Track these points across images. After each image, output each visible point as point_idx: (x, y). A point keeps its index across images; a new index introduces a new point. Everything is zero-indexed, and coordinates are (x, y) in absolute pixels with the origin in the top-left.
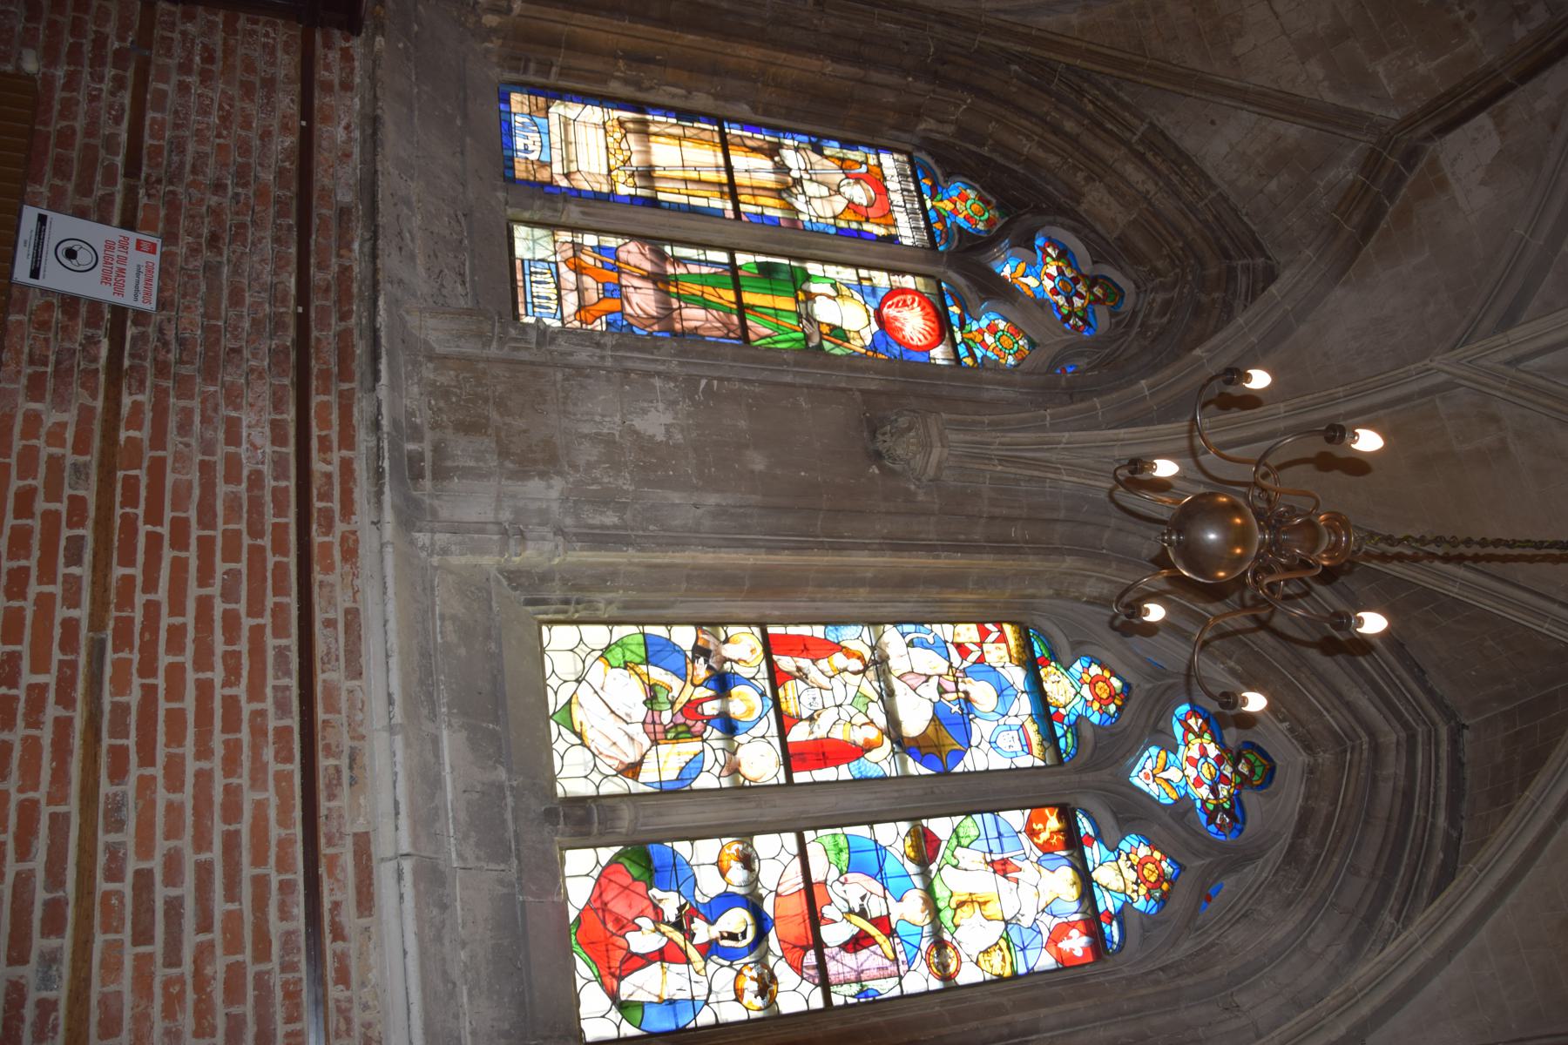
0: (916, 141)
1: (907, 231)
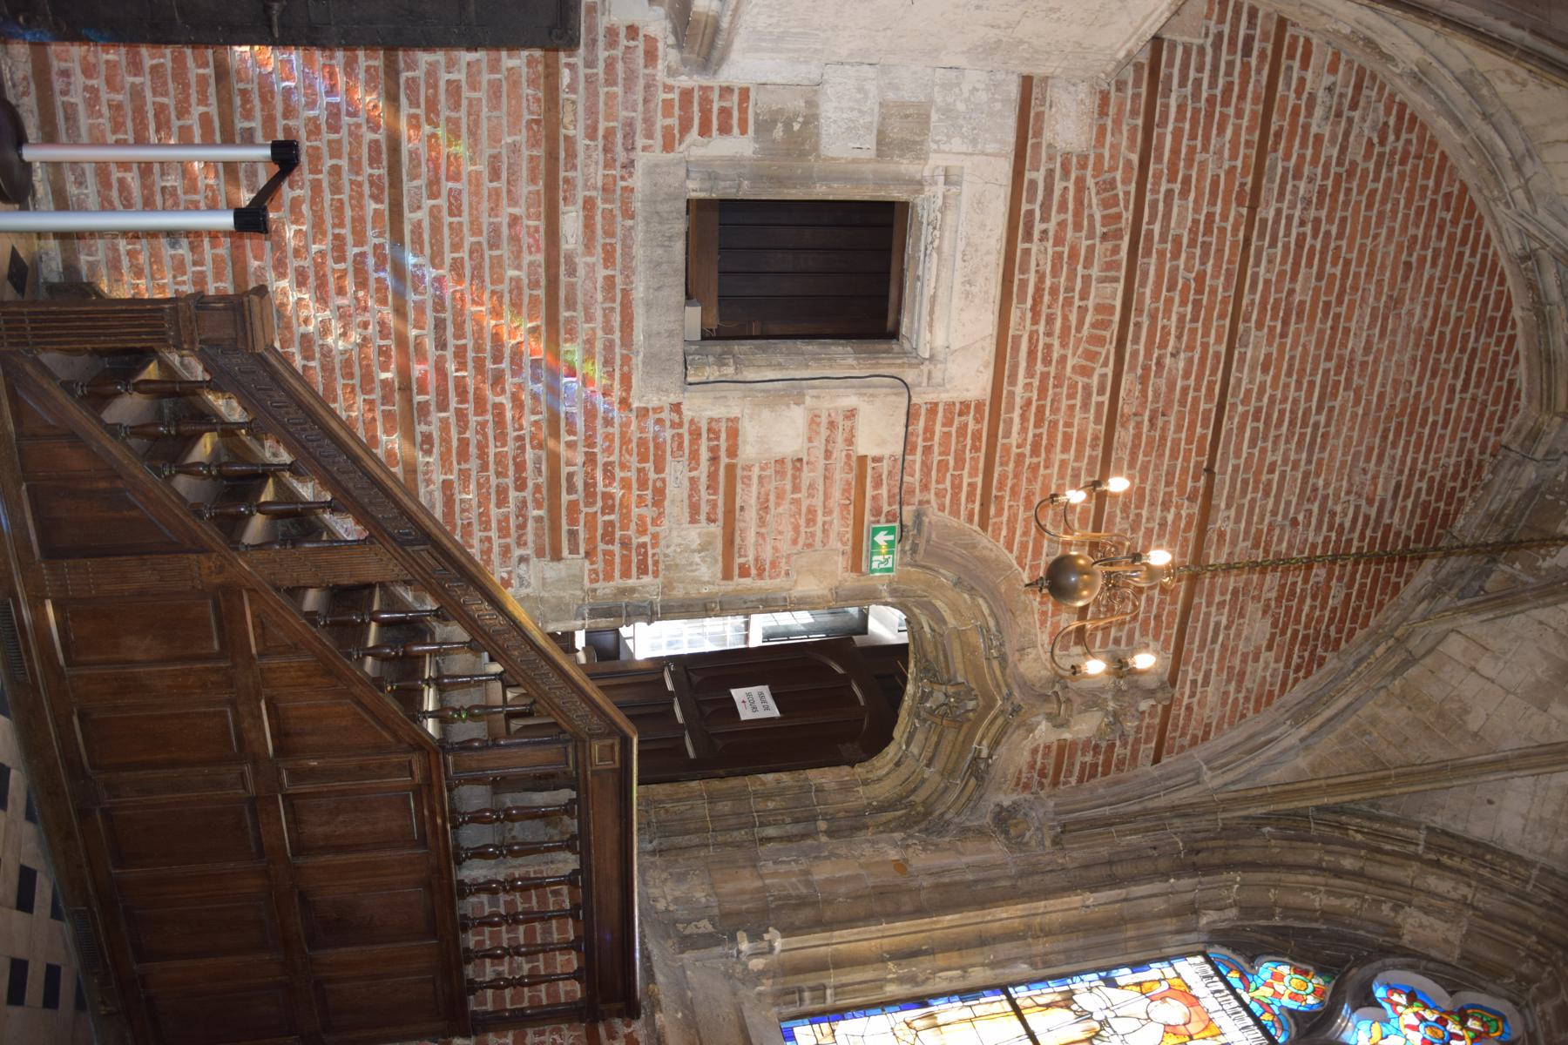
0: (1204, 938)
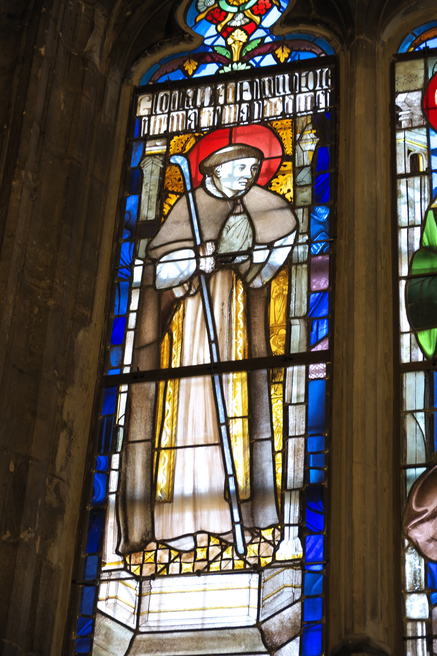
0: (116, 75)
1: (309, 96)
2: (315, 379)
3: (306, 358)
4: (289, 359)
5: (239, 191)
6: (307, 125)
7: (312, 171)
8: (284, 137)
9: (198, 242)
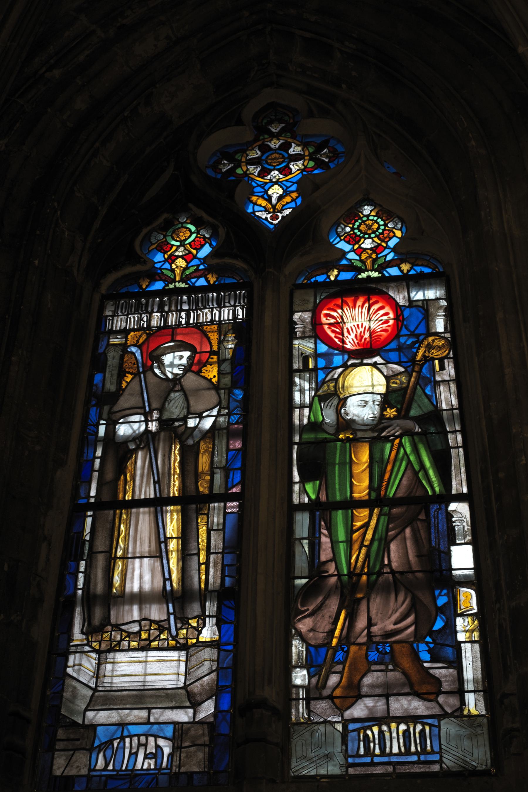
2: (231, 513)
3: (225, 498)
4: (212, 497)
5: (179, 374)
6: (229, 330)
7: (232, 364)
8: (212, 337)
9: (147, 410)
